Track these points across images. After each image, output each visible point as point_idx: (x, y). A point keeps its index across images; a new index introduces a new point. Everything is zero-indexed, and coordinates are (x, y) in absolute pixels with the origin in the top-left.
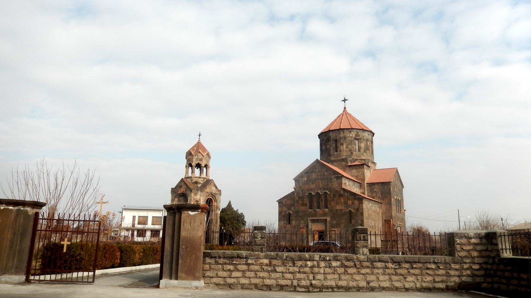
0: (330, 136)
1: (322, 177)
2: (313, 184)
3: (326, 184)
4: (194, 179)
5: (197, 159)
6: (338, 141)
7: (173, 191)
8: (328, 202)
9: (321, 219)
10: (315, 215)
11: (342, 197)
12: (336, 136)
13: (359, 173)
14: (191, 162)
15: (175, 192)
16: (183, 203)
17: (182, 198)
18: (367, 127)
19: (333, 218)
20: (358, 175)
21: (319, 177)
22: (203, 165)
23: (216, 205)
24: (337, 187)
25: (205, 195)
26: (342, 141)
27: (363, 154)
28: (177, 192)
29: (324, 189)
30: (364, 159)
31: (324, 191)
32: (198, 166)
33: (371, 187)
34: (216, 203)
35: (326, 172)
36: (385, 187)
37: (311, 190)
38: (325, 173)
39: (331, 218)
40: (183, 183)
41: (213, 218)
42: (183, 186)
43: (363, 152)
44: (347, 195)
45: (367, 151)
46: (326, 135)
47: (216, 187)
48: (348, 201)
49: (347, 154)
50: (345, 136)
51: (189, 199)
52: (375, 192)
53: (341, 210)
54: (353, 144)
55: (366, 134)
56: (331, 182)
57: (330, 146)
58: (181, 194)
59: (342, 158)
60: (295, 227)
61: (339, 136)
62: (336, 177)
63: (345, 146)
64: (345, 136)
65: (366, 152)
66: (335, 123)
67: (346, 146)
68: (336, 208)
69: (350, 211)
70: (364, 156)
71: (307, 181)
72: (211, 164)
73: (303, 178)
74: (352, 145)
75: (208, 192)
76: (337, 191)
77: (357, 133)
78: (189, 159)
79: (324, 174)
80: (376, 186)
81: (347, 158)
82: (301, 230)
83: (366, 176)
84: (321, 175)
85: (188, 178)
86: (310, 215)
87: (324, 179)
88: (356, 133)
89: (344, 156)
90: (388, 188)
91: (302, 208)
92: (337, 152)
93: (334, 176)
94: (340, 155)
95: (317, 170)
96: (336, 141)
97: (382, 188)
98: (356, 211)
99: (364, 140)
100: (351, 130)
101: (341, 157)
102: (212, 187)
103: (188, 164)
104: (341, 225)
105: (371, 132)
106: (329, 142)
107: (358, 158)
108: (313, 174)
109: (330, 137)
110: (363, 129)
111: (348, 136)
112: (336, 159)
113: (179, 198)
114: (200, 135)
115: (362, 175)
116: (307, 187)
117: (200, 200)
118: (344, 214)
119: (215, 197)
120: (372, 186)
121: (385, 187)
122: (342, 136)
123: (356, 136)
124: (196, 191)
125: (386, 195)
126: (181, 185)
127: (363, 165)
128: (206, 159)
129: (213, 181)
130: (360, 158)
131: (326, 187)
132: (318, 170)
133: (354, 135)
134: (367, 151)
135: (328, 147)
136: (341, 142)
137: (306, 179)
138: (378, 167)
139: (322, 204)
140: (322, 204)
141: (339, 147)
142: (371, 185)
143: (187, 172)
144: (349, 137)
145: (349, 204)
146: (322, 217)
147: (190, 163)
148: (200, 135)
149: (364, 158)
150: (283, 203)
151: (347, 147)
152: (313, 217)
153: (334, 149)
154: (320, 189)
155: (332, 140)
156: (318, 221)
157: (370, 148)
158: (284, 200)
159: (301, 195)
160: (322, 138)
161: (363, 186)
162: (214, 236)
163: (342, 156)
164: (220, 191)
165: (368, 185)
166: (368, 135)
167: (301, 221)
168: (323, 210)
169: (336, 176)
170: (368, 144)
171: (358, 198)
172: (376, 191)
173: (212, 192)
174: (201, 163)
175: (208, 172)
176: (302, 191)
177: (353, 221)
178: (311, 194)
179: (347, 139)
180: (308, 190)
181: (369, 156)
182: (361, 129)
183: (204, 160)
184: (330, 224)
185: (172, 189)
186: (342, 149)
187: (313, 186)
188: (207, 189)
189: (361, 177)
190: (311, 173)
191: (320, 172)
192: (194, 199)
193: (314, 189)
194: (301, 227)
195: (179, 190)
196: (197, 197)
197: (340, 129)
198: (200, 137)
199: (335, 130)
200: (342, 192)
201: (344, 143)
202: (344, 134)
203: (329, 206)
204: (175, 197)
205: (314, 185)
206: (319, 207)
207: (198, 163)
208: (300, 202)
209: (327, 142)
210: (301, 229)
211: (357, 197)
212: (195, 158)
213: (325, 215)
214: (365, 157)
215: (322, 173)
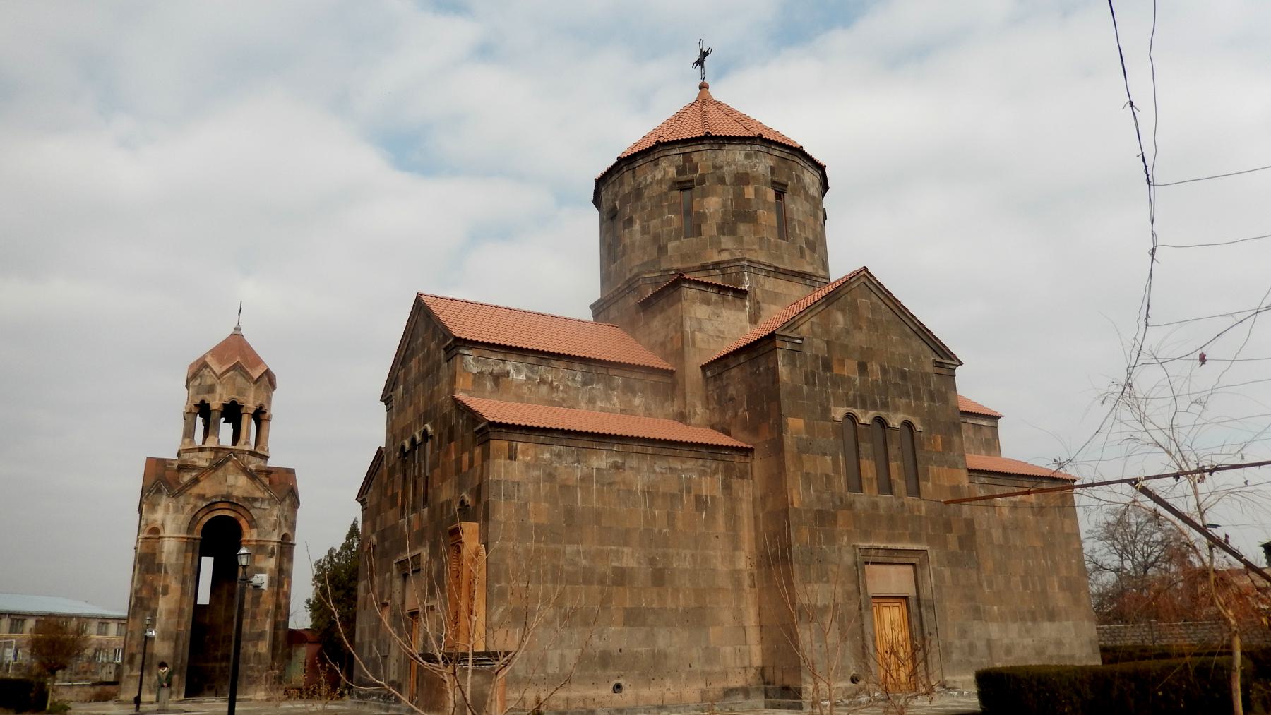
30: (717, 265)
32: (233, 412)
43: (715, 232)
64: (640, 183)
65: (733, 232)
77: (685, 161)
88: (679, 160)
90: (768, 369)
94: (624, 270)
107: (690, 265)
117: (163, 525)
123: (680, 171)
124: (156, 496)
130: (699, 263)
133: (672, 172)
134: (742, 228)
144: (651, 183)
151: (644, 231)
166: (748, 156)
181: (755, 247)
183: (219, 389)
188: (201, 484)
202: (634, 177)
207: (203, 402)
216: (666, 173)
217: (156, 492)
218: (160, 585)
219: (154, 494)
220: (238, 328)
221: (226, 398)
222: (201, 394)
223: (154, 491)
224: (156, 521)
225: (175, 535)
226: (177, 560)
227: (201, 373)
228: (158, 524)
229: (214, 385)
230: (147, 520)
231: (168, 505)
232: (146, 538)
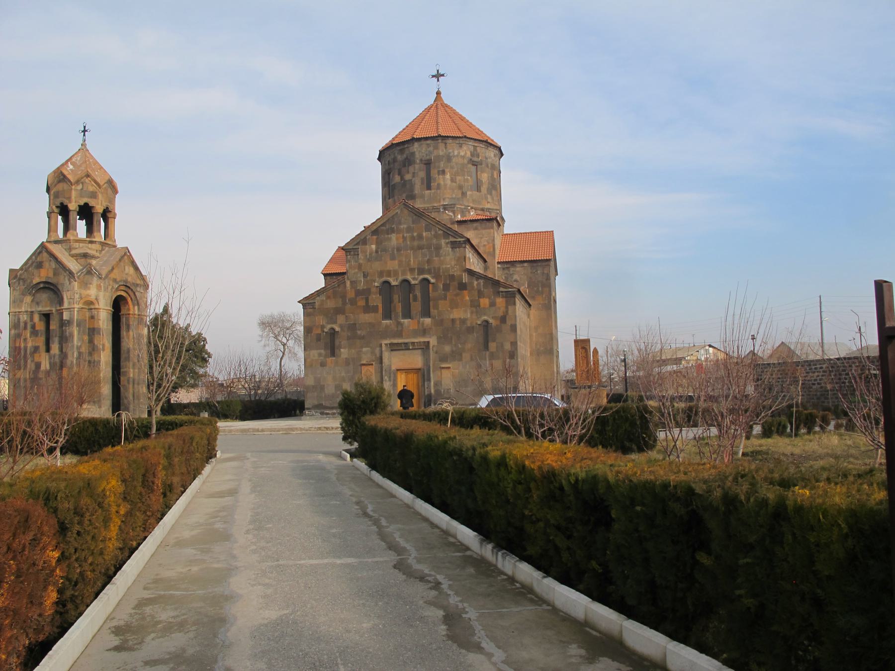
0: (414, 152)
1: (416, 243)
2: (393, 258)
3: (426, 259)
4: (77, 245)
5: (81, 194)
6: (432, 166)
7: (15, 277)
8: (431, 303)
9: (413, 343)
10: (400, 334)
11: (466, 289)
12: (427, 152)
13: (481, 238)
14: (66, 202)
15: (24, 280)
16: (48, 309)
17: (44, 296)
18: (491, 138)
19: (444, 339)
20: (479, 243)
21: (408, 243)
22: (99, 209)
23: (136, 312)
24: (453, 268)
25: (110, 287)
26: (442, 164)
27: (486, 198)
28: (29, 281)
29: (421, 271)
30: (488, 210)
31: (421, 277)
32: (86, 212)
33: (506, 271)
34: (136, 307)
35: (426, 231)
36: (539, 272)
37: (389, 274)
38: (424, 234)
39: (439, 338)
40: (45, 255)
41: (131, 346)
42: (46, 265)
43: (486, 192)
44: (477, 285)
45: (494, 192)
46: (402, 152)
47: (136, 269)
48: (482, 300)
49: (454, 196)
50: (450, 153)
51: (65, 297)
52: (515, 281)
53: (463, 321)
54: (466, 174)
55: (491, 153)
56: (438, 255)
57: (413, 177)
58: (42, 286)
59: (442, 203)
60: (347, 362)
61: (435, 153)
62: (452, 243)
63: (448, 176)
64: (450, 153)
65: (491, 194)
66: (422, 124)
67: (450, 176)
68: (452, 317)
69: (487, 321)
70: (488, 202)
71: (377, 252)
72: (120, 207)
73: (366, 244)
74: (464, 175)
75: (118, 280)
76: (452, 277)
78: (58, 192)
79: (420, 237)
80: (518, 269)
81: (455, 205)
82: (364, 369)
83: (496, 247)
84: (413, 238)
85: (57, 242)
86: (385, 334)
87: (420, 248)
89: (447, 200)
90: (543, 273)
91: (366, 318)
92: (431, 190)
93: (447, 241)
94: (439, 197)
95: (402, 227)
96: (428, 164)
97: (531, 273)
98: (498, 323)
99: (487, 166)
100: (461, 142)
101: (440, 202)
102: (127, 268)
103: (57, 207)
104: (464, 355)
105: (499, 149)
106: (410, 164)
107: (478, 206)
108: (393, 236)
109: (413, 154)
110: (486, 142)
111: (456, 153)
112: (429, 206)
113: (34, 295)
114: (85, 131)
115: (489, 243)
116: (377, 266)
118: (470, 330)
119: (134, 293)
120: (509, 268)
121: (537, 271)
122: (441, 153)
123: (472, 155)
124: (87, 276)
125: (540, 289)
126: (38, 259)
127: (490, 220)
128: (107, 194)
129: (129, 251)
130: (481, 207)
131: (427, 267)
132: (405, 226)
133: (469, 154)
134: (494, 192)
135: (408, 177)
136: (439, 167)
137: (374, 247)
138: (508, 229)
139: (416, 307)
140: (416, 307)
141: (435, 179)
142: (508, 265)
143: (51, 229)
144: (457, 156)
145: (482, 306)
146: (415, 337)
147: (62, 204)
148: (85, 131)
149: (488, 206)
150: (317, 307)
151: (452, 180)
152: (394, 336)
153: (422, 183)
154: (412, 270)
155: (418, 161)
156: (406, 347)
157: (498, 186)
158: (318, 298)
159: (361, 286)
160: (393, 157)
161: (491, 267)
162: (136, 391)
163: (442, 200)
164: (143, 278)
165: (499, 266)
166: (495, 156)
167: (362, 347)
168: (419, 322)
169: (452, 239)
170: (495, 176)
171: (506, 292)
172: (518, 279)
173: (126, 281)
174: (92, 203)
175: (113, 229)
176: (365, 276)
177: (493, 346)
178: (387, 282)
179: (454, 160)
180: (381, 274)
182: (480, 140)
183: (100, 196)
184: (436, 353)
185: (11, 271)
186: (442, 183)
187: (392, 265)
189: (487, 247)
190: (388, 234)
191: (409, 230)
192: (81, 298)
193: (396, 273)
194: (364, 362)
195: (33, 275)
196: (88, 292)
197: (440, 136)
198: (84, 135)
199: (426, 139)
200: (465, 278)
201: (447, 170)
202: (446, 148)
203: (433, 312)
204: (23, 294)
205: (396, 262)
206: (407, 314)
207: (86, 204)
208: (361, 303)
209: (404, 166)
210: (363, 367)
211: (502, 289)
212: (76, 190)
213: (424, 332)
214: (489, 204)
215: (415, 234)
216: (466, 153)
217: (86, 274)
218: (100, 344)
219: (84, 275)
220: (84, 145)
221: (105, 204)
222: (83, 197)
223: (85, 273)
224: (90, 296)
225: (107, 308)
226: (107, 326)
227: (82, 180)
228: (93, 298)
229: (96, 192)
230: (81, 294)
231: (100, 284)
232: (82, 308)
